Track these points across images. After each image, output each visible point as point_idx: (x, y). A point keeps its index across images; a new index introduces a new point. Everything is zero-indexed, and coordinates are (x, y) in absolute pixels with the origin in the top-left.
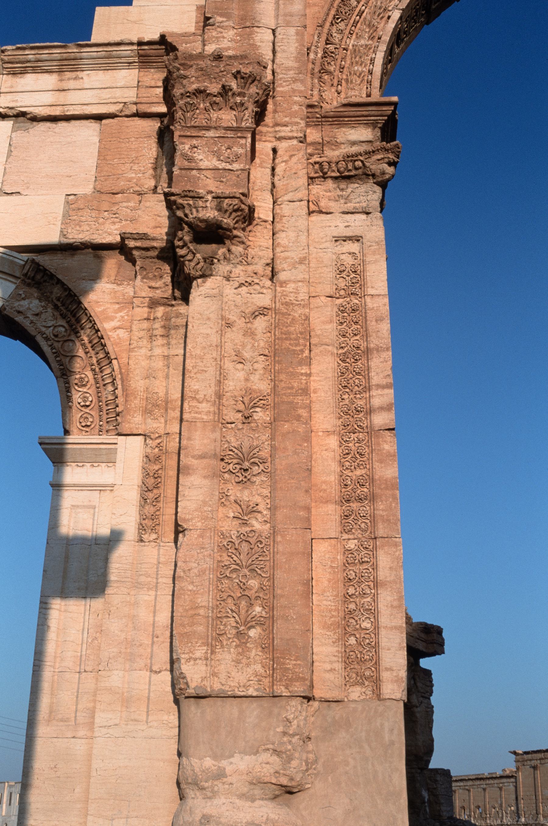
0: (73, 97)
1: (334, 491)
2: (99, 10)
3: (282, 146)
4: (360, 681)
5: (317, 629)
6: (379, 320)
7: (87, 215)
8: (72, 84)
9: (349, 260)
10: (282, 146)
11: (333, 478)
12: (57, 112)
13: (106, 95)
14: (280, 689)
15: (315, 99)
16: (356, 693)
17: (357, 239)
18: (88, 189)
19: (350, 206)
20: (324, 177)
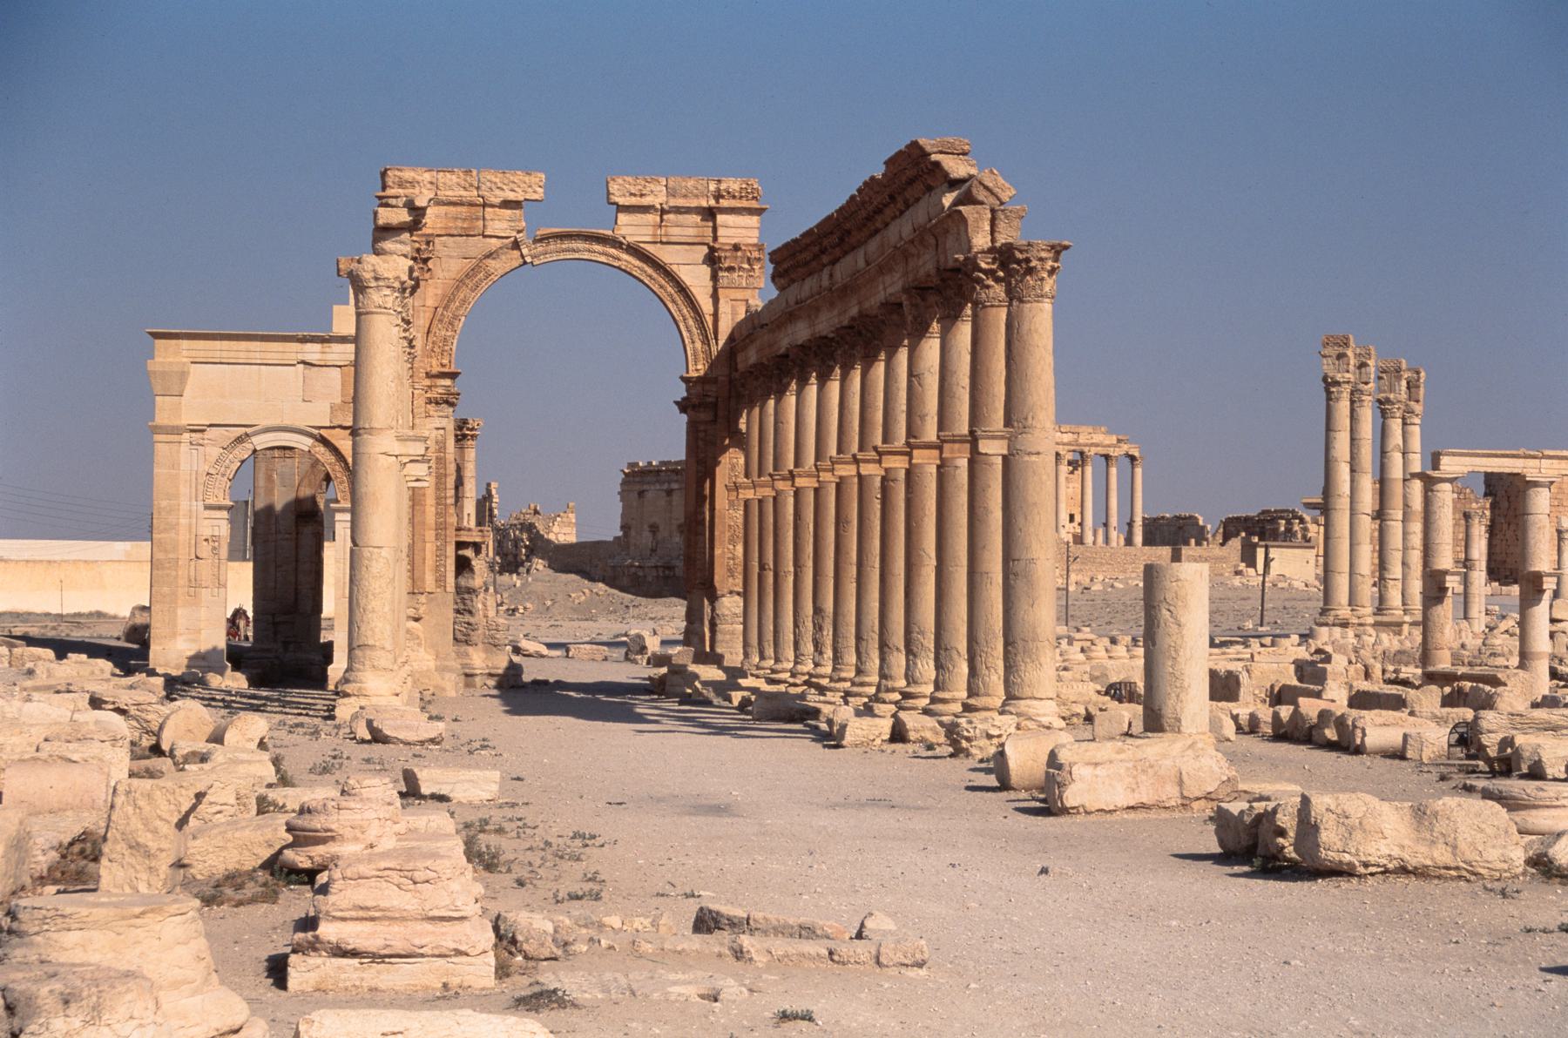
0: (329, 357)
1: (434, 526)
2: (336, 308)
3: (416, 392)
4: (440, 587)
5: (427, 571)
6: (450, 463)
7: (339, 413)
8: (327, 350)
9: (440, 438)
10: (416, 392)
11: (433, 522)
12: (322, 363)
13: (343, 356)
14: (416, 591)
15: (429, 369)
16: (438, 590)
17: (443, 429)
18: (338, 401)
19: (441, 414)
20: (430, 403)
